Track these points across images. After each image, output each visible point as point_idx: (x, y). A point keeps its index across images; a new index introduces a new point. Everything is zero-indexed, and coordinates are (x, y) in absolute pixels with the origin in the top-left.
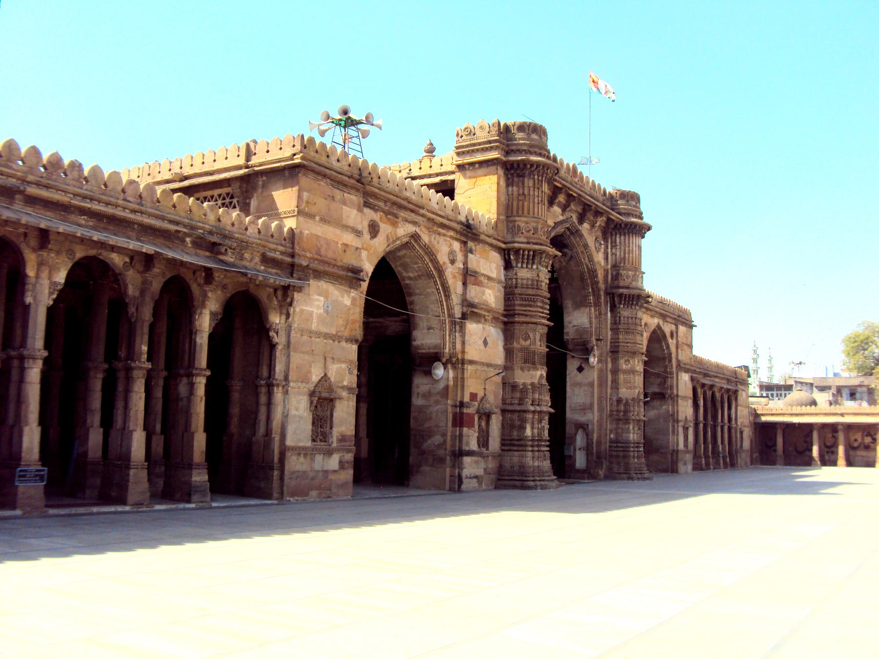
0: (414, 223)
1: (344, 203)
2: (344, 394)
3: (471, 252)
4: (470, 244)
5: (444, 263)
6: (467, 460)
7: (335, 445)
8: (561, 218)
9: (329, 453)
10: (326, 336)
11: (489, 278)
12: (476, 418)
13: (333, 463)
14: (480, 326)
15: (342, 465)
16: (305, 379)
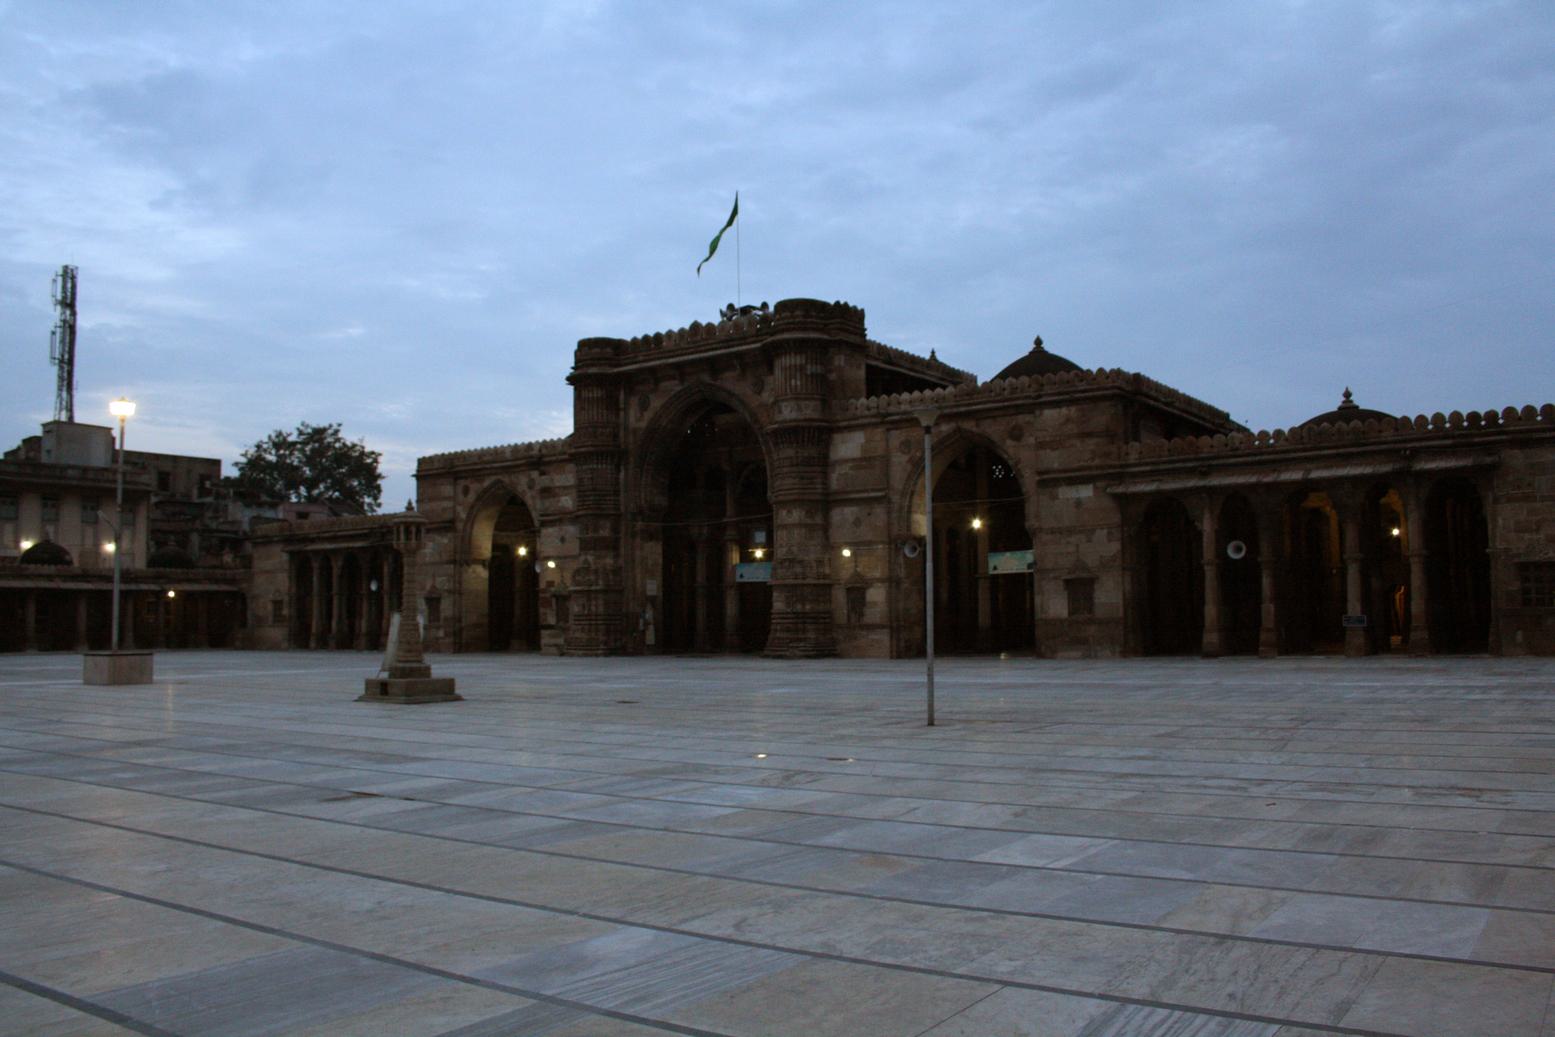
0: (496, 474)
1: (442, 484)
2: (446, 594)
3: (543, 473)
4: (542, 468)
5: (524, 491)
6: (544, 633)
7: (441, 623)
8: (679, 388)
9: (438, 628)
10: (434, 564)
11: (565, 488)
12: (554, 601)
13: (441, 633)
14: (556, 529)
15: (446, 635)
16: (423, 588)
